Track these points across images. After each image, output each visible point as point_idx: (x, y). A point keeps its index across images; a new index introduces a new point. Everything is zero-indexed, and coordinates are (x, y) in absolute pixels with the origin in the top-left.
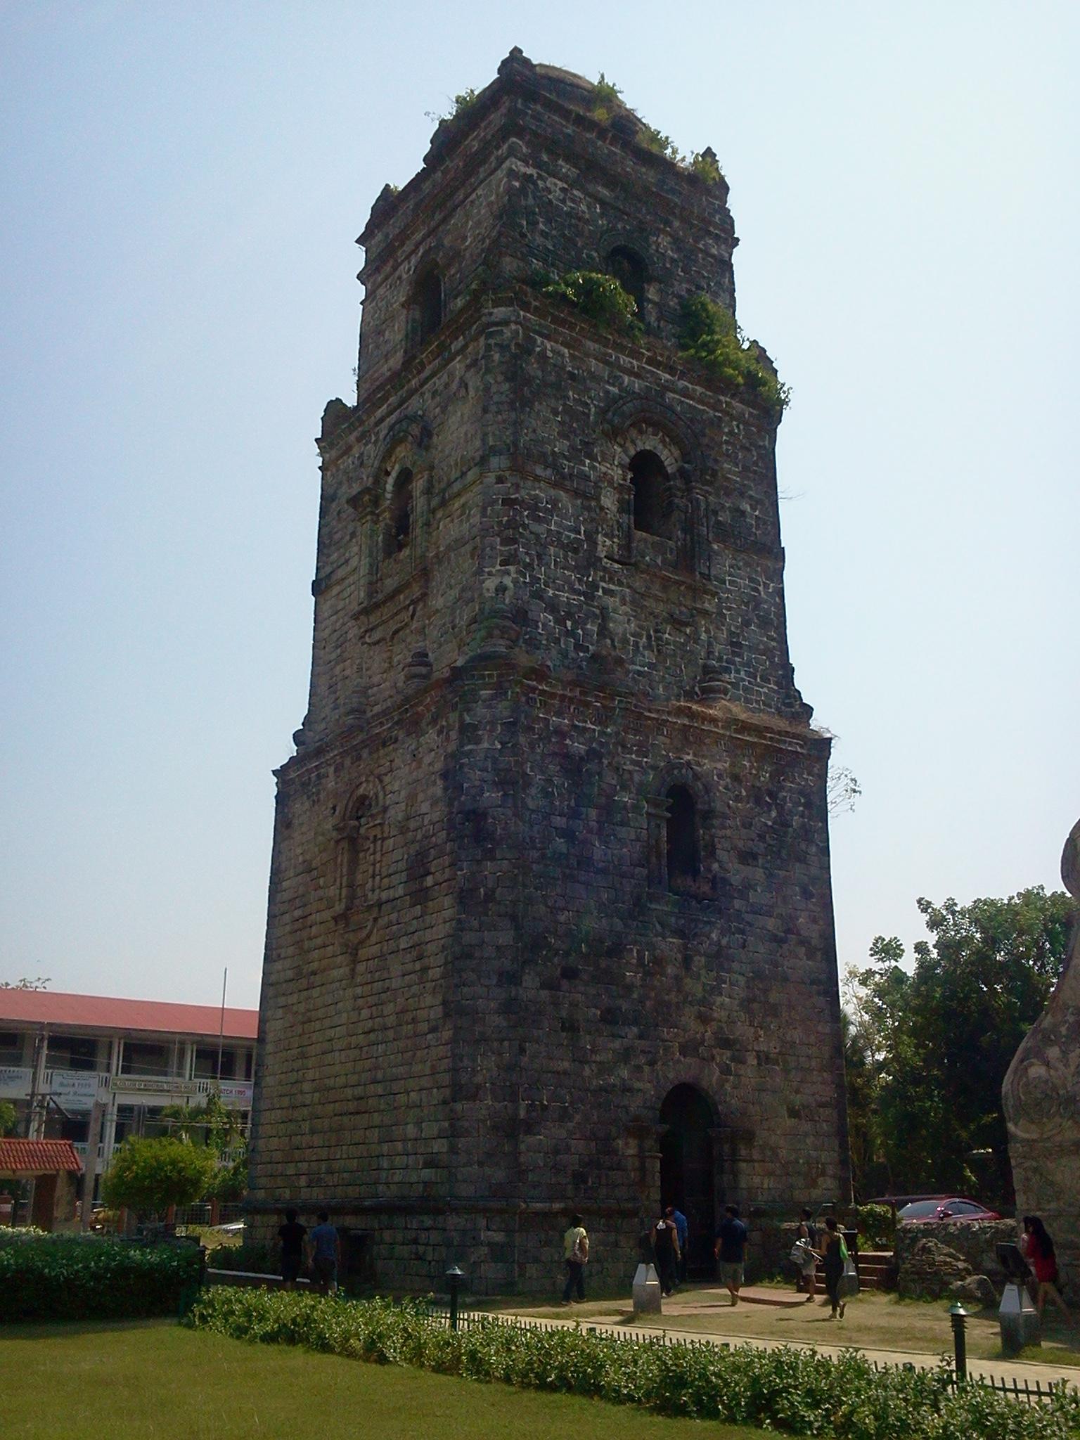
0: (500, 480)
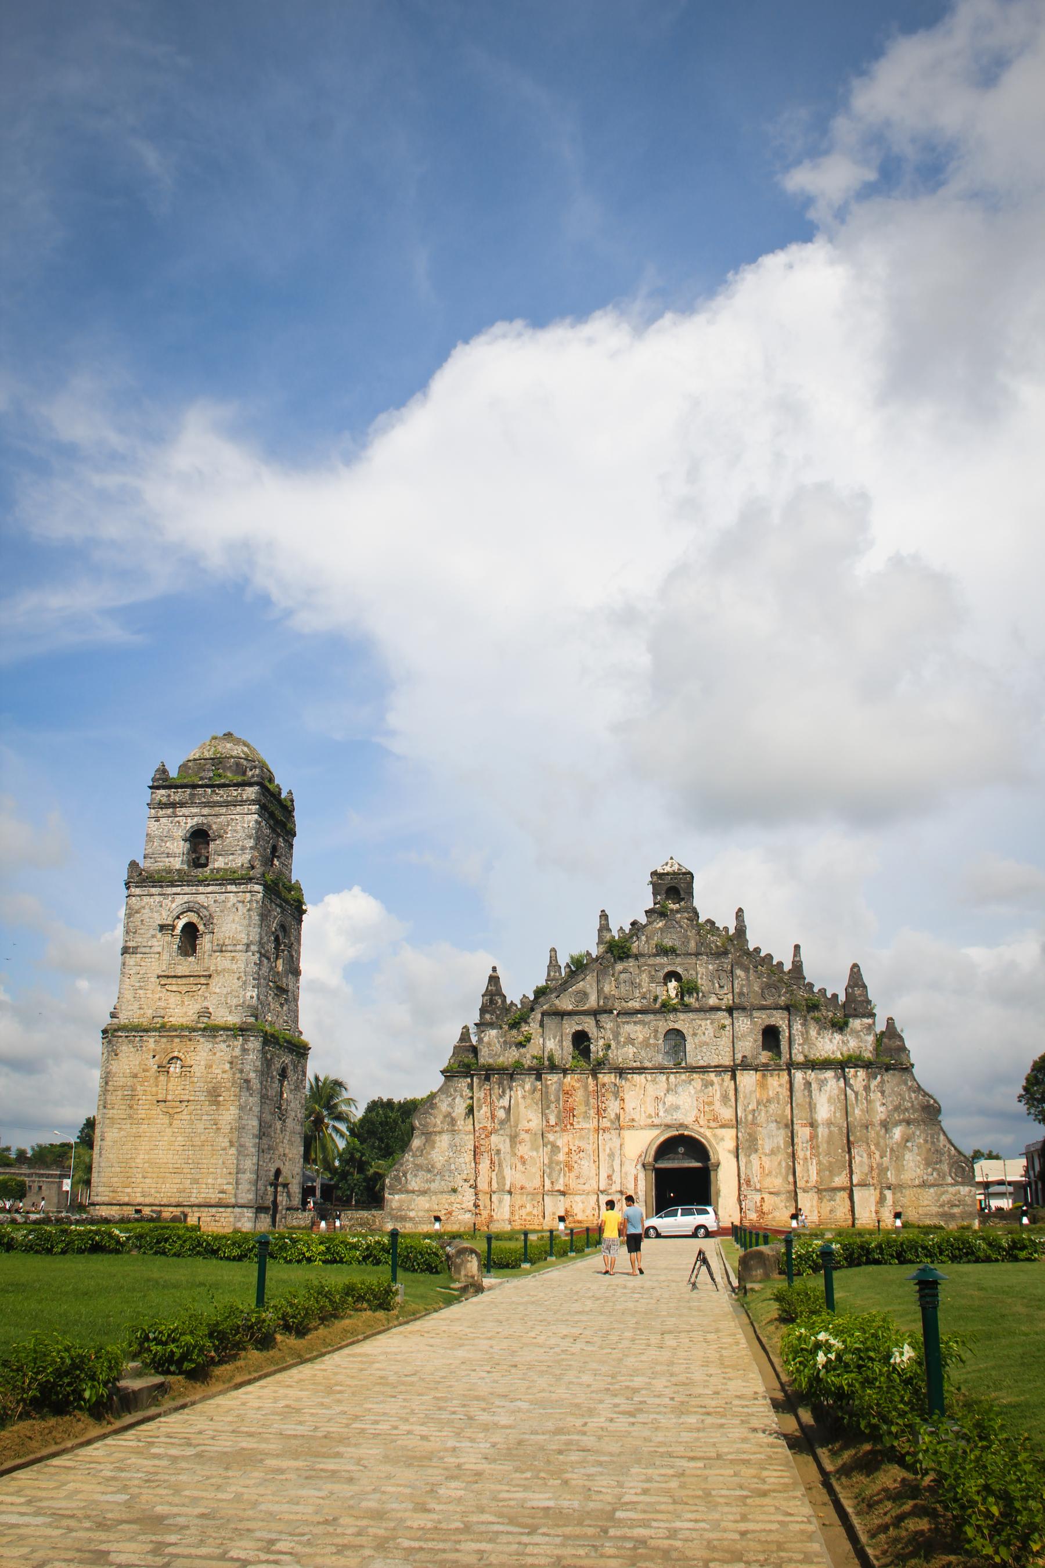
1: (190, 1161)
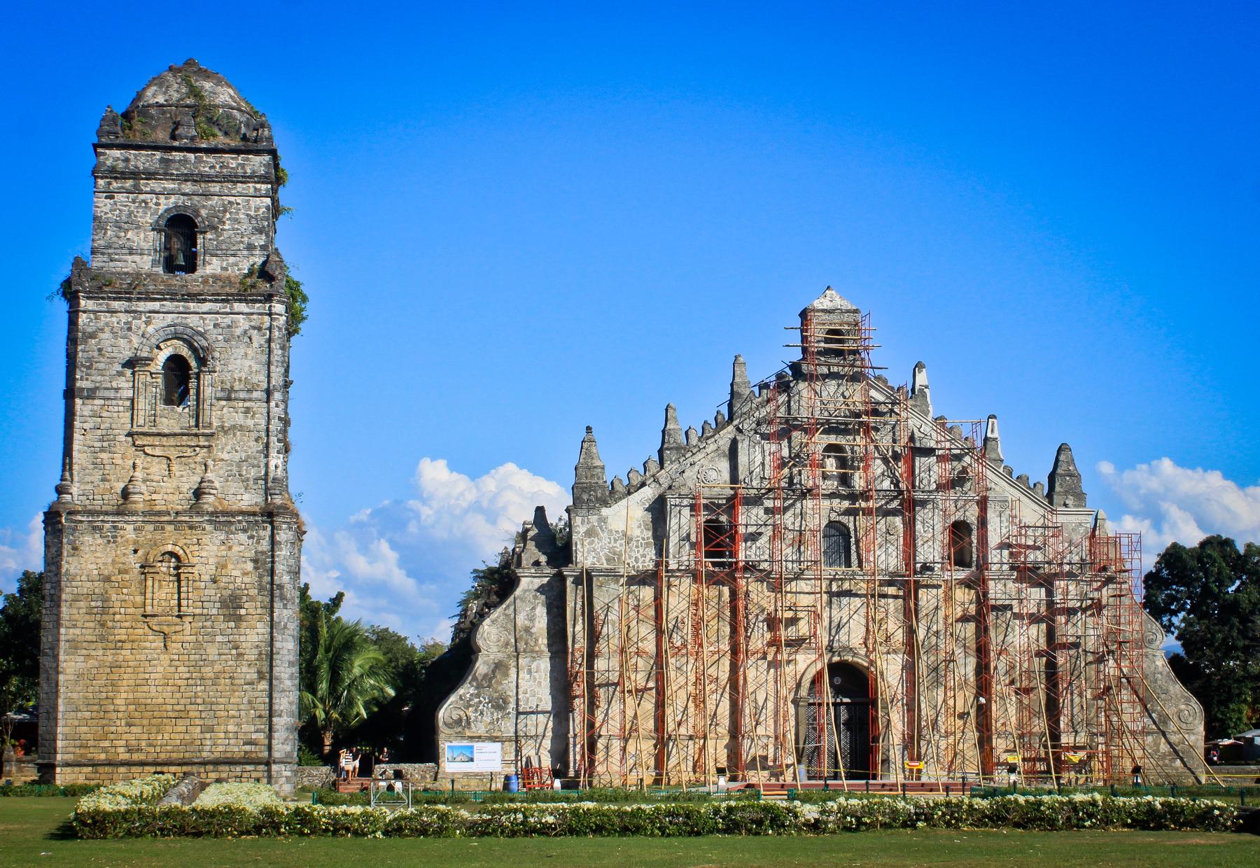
0: (277, 406)
1: (199, 701)
